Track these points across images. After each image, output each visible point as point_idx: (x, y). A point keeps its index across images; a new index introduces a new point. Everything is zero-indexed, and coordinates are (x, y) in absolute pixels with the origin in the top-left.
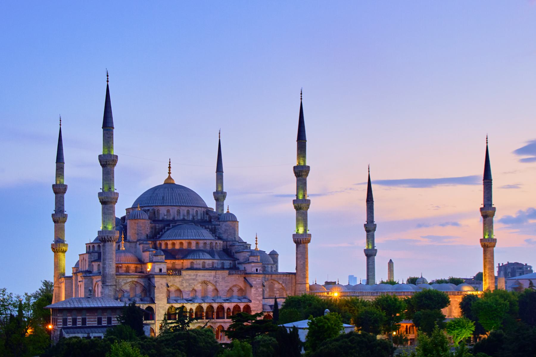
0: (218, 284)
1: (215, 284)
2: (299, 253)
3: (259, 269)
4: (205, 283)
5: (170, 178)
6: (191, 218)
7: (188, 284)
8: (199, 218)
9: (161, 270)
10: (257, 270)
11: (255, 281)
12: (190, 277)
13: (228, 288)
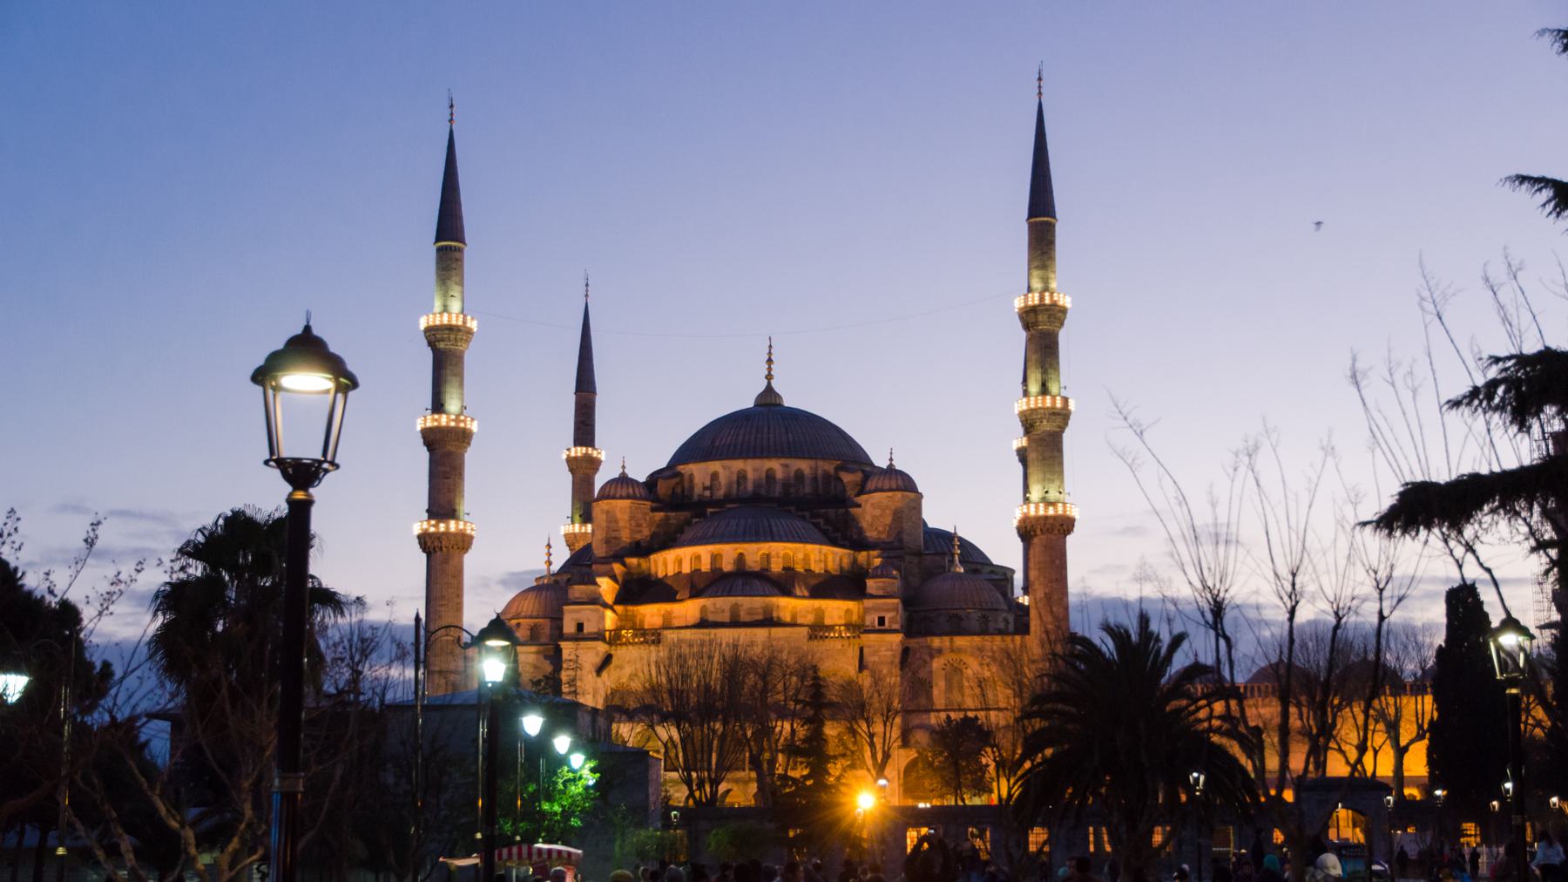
2: (1031, 565)
3: (888, 616)
5: (769, 390)
6: (778, 490)
8: (808, 490)
9: (580, 627)
10: (882, 621)
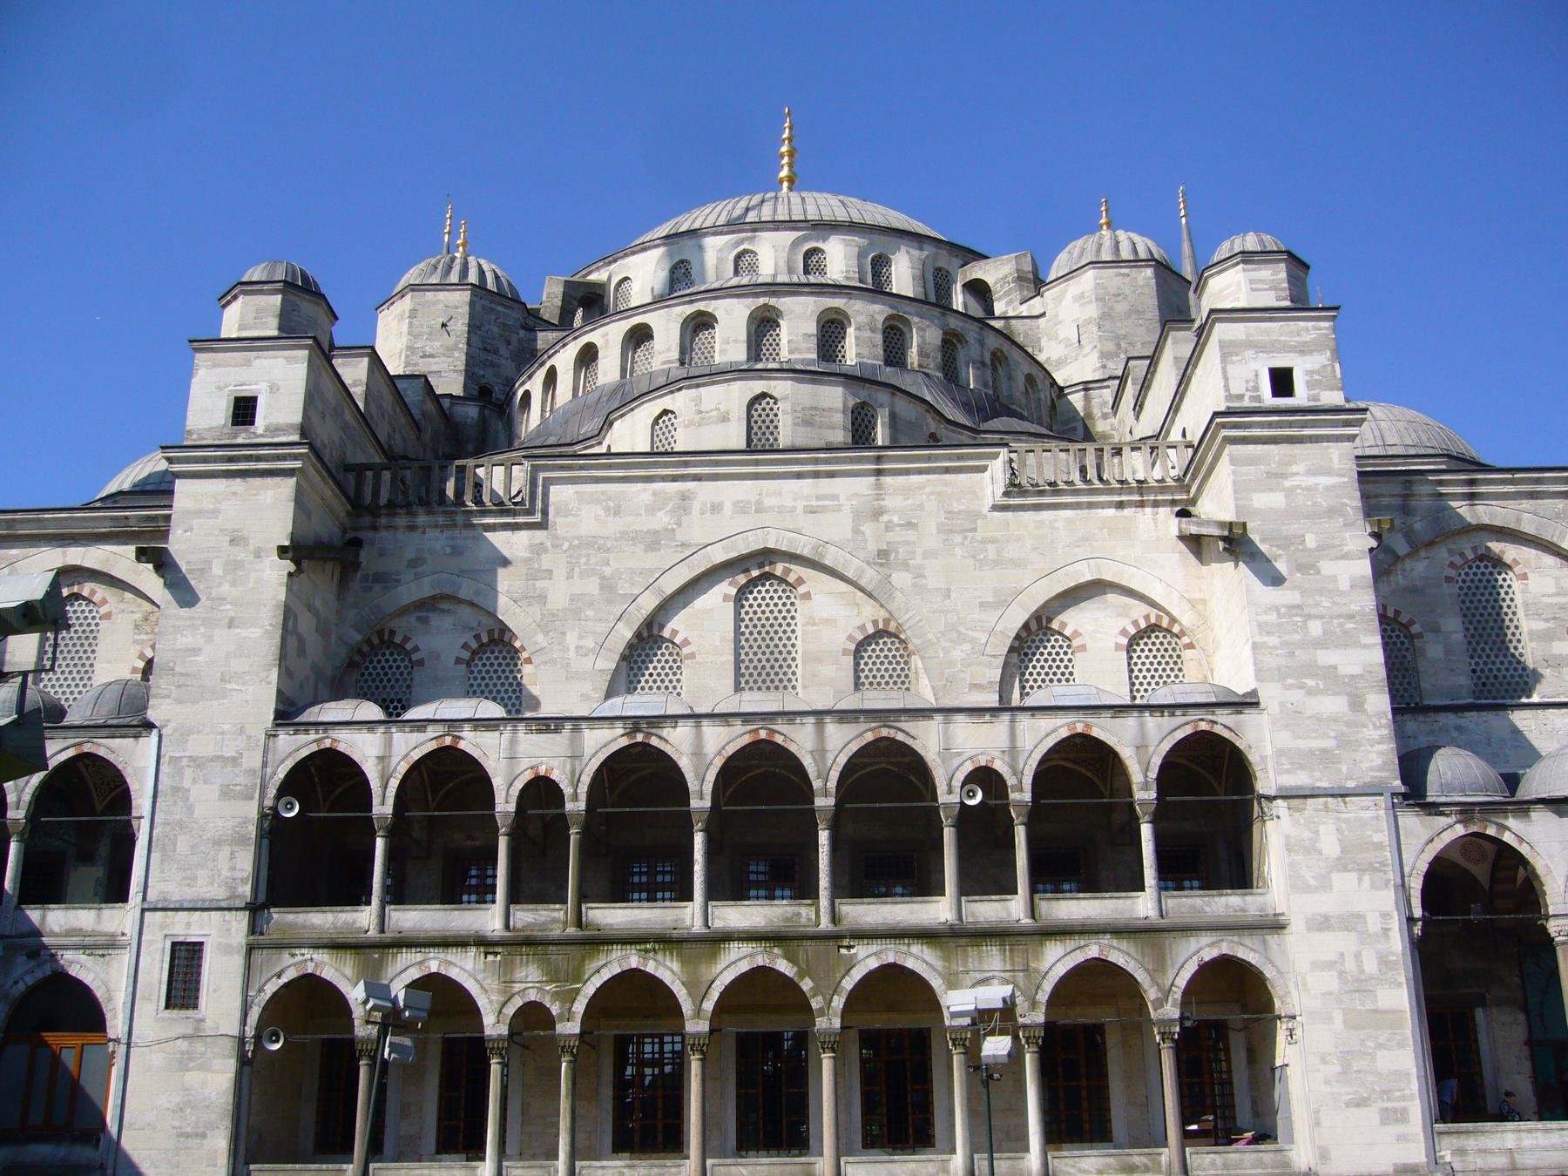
0: (900, 578)
1: (869, 577)
4: (758, 568)
7: (592, 587)
10: (1282, 381)
11: (1275, 478)
12: (615, 525)
13: (1017, 618)
